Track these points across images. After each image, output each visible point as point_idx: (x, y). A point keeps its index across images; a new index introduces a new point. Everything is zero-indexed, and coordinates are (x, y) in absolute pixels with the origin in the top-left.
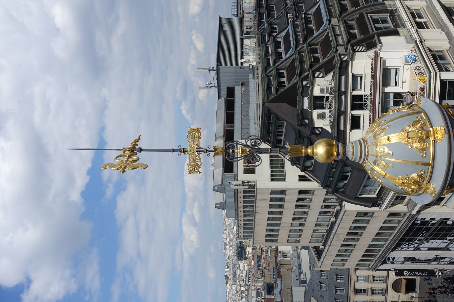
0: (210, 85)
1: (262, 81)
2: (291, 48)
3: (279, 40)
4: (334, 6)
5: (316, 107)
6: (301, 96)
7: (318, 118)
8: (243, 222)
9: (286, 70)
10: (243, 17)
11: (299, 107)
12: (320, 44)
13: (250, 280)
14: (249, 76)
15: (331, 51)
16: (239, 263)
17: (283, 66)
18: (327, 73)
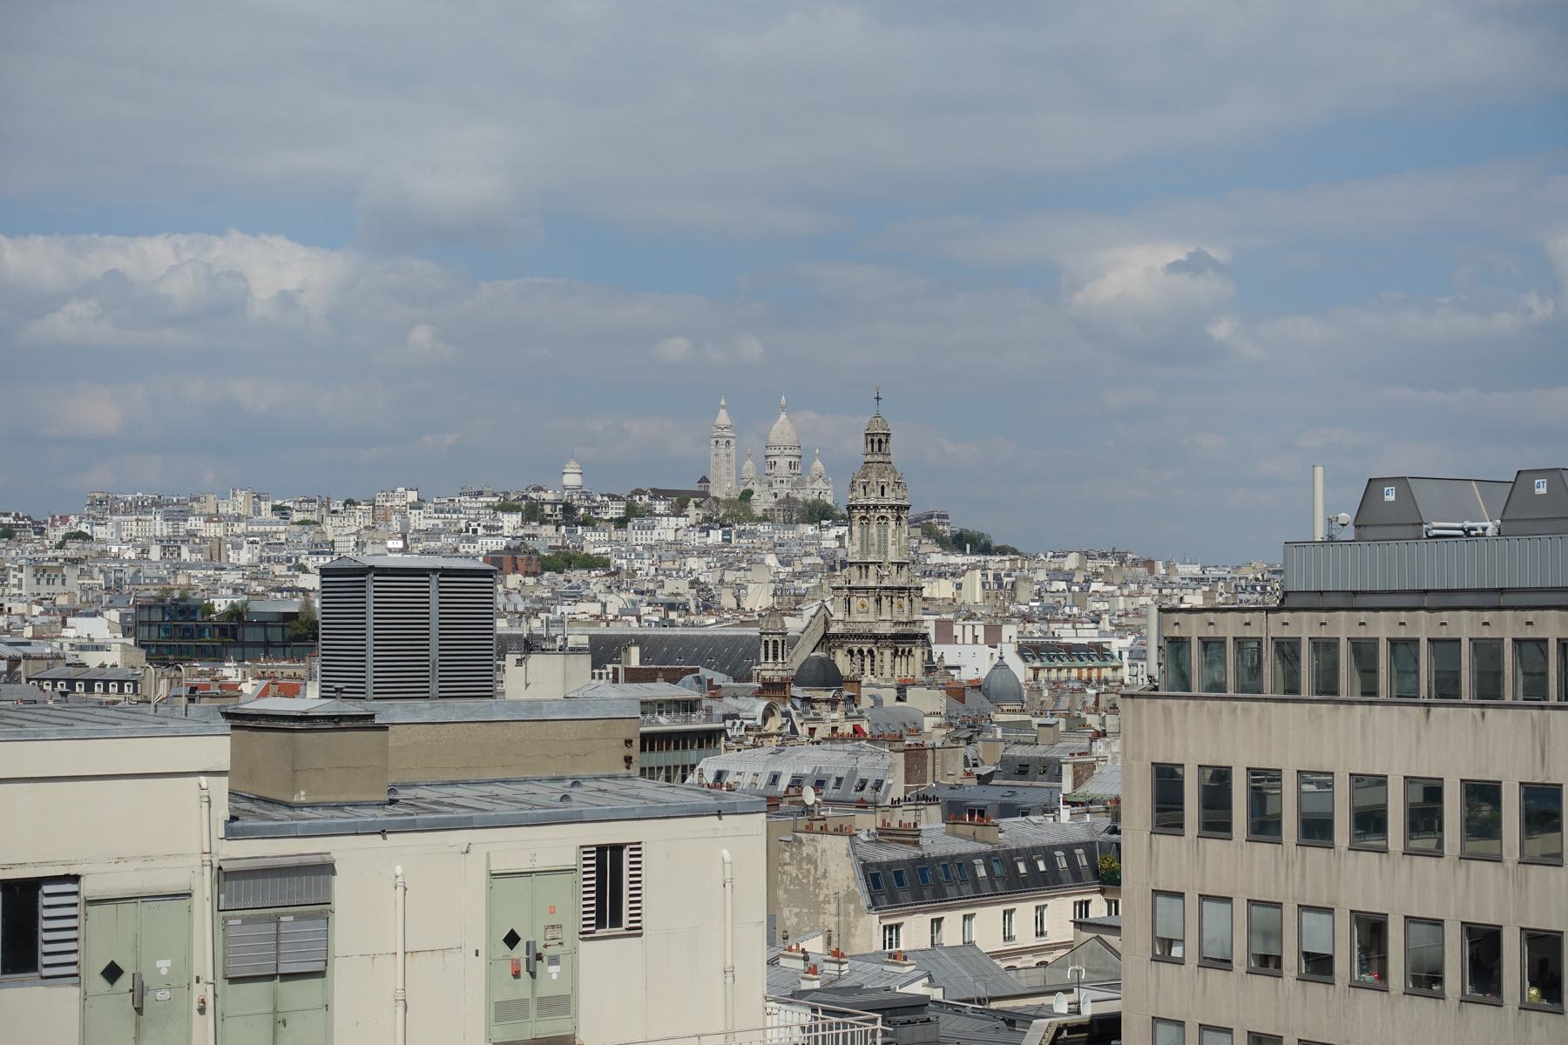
8: (1305, 635)
13: (113, 689)
16: (106, 614)
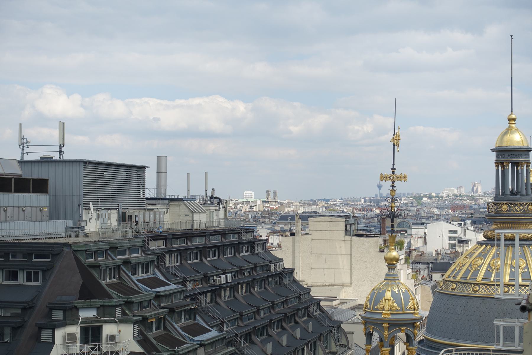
0: (25, 145)
1: (95, 241)
2: (152, 289)
3: (151, 269)
4: (216, 352)
5: (85, 331)
6: (99, 305)
7: (69, 335)
9: (119, 281)
10: (145, 209)
11: (82, 303)
12: (167, 333)
14: (70, 220)
15: (168, 348)
17: (124, 276)
18: (139, 342)
